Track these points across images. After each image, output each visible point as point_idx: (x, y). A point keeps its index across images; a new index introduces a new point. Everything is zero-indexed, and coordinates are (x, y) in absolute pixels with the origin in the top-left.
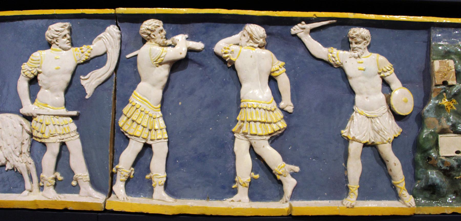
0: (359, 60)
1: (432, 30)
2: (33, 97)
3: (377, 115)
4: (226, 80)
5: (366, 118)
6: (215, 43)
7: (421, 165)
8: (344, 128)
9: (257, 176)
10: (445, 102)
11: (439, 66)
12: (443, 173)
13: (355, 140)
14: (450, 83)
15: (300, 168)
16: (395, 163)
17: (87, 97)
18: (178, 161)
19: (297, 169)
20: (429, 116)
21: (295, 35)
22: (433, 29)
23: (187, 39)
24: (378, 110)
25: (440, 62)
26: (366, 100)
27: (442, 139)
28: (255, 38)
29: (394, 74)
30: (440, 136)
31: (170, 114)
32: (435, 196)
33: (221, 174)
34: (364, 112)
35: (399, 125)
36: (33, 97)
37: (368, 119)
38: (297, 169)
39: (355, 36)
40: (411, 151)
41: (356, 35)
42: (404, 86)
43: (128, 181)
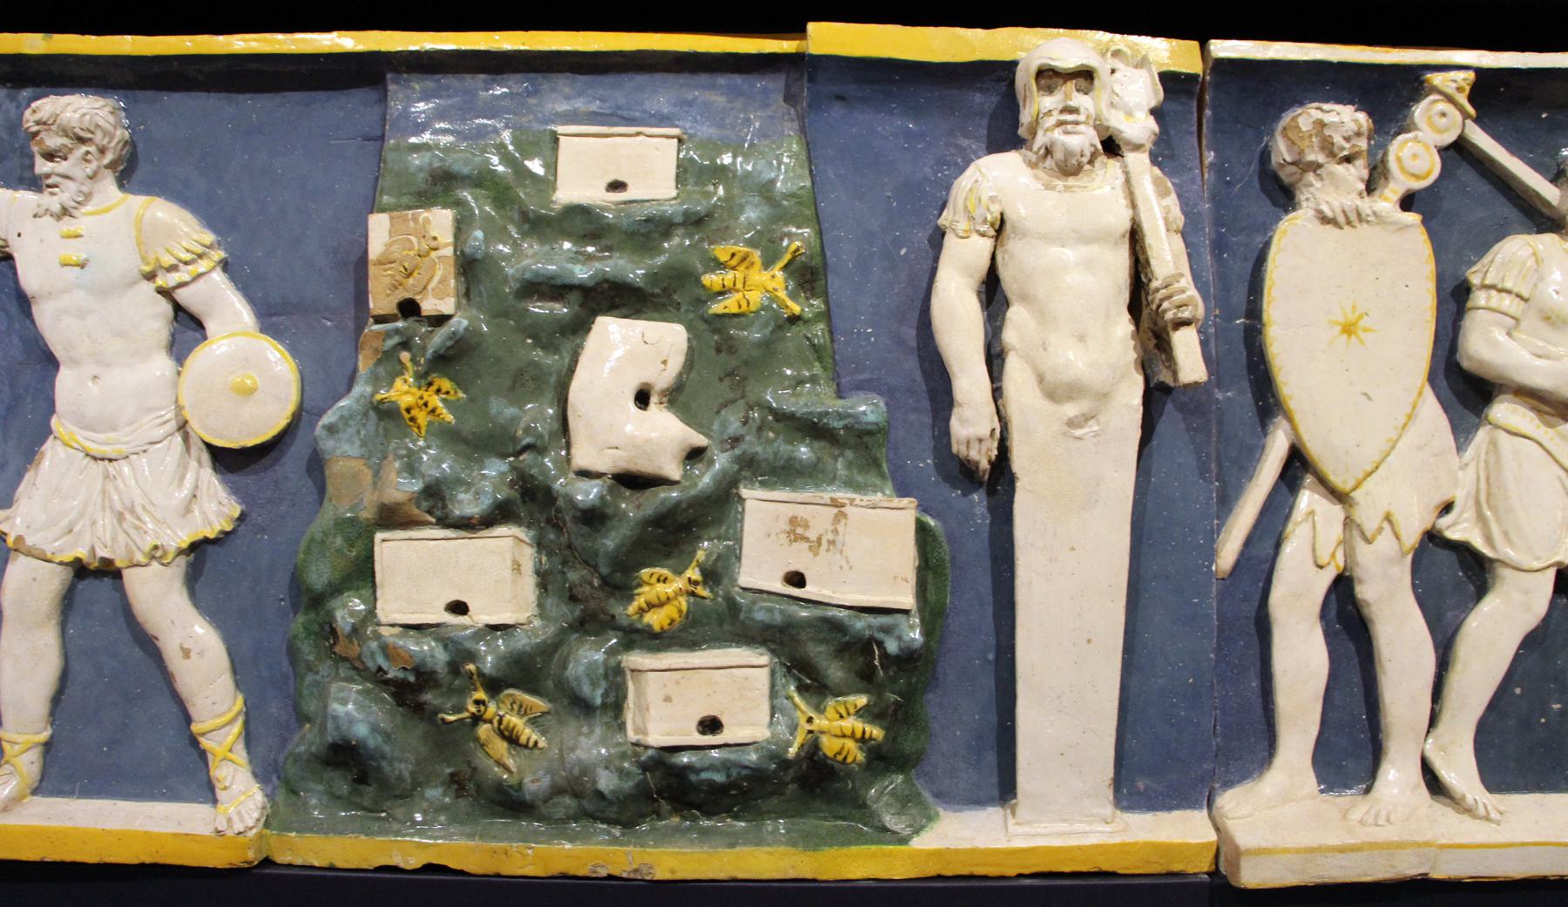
0: (68, 225)
1: (392, 87)
3: (125, 449)
5: (88, 459)
7: (311, 658)
10: (403, 392)
11: (386, 234)
12: (393, 695)
13: (22, 550)
14: (429, 306)
16: (186, 646)
20: (338, 452)
22: (396, 82)
24: (136, 425)
25: (391, 218)
26: (90, 384)
27: (391, 550)
29: (218, 277)
30: (379, 536)
32: (370, 791)
34: (81, 440)
35: (235, 490)
37: (93, 465)
39: (35, 129)
40: (282, 600)
41: (38, 123)
42: (264, 329)
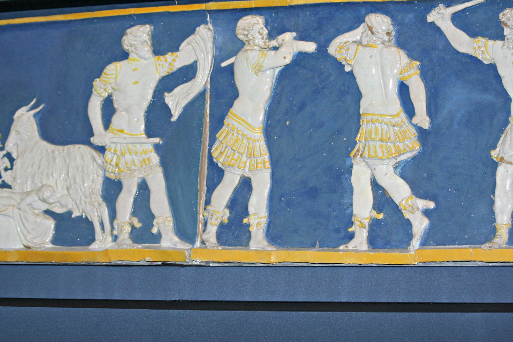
2: (107, 123)
4: (344, 89)
6: (329, 41)
8: (494, 147)
9: (381, 216)
15: (435, 203)
17: (174, 119)
18: (283, 199)
19: (431, 205)
21: (433, 24)
23: (295, 39)
28: (376, 31)
31: (276, 137)
33: (335, 213)
36: (107, 123)
38: (431, 205)
43: (222, 226)
